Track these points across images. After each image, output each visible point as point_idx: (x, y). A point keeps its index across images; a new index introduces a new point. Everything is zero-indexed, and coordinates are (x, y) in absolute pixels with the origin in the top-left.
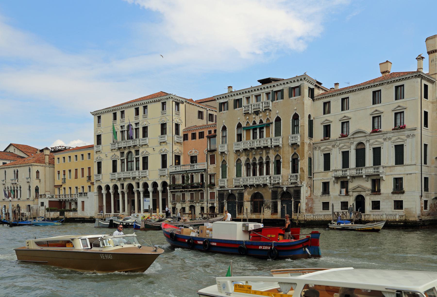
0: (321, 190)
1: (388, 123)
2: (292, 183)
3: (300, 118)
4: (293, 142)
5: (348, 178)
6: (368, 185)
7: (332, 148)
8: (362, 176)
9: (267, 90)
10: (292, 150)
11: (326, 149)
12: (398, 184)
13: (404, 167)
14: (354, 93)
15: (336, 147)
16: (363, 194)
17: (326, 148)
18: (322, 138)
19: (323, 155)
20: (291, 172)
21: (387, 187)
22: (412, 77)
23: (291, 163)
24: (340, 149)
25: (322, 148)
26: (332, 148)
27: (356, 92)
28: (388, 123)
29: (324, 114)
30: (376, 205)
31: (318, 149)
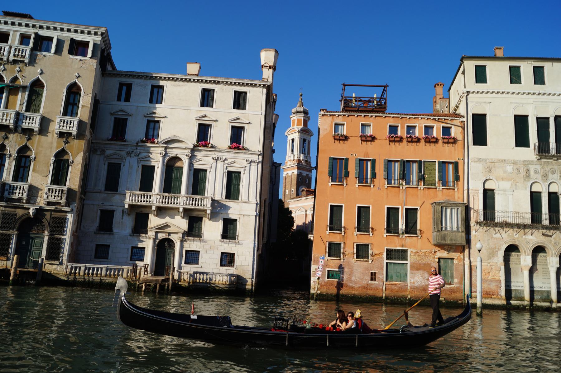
0: (97, 223)
1: (220, 136)
2: (49, 204)
3: (82, 92)
4: (64, 130)
5: (154, 208)
6: (180, 223)
7: (126, 156)
8: (179, 208)
9: (24, 30)
10: (58, 143)
11: (115, 156)
12: (229, 230)
13: (240, 204)
14: (173, 82)
15: (133, 155)
16: (172, 237)
17: (115, 154)
18: (110, 136)
19: (107, 164)
20: (49, 182)
21: (212, 229)
22: (260, 85)
23: (52, 165)
24: (140, 160)
25: (108, 152)
26: (126, 156)
27: (177, 83)
28: (220, 136)
29: (119, 99)
30: (192, 257)
31: (99, 153)
